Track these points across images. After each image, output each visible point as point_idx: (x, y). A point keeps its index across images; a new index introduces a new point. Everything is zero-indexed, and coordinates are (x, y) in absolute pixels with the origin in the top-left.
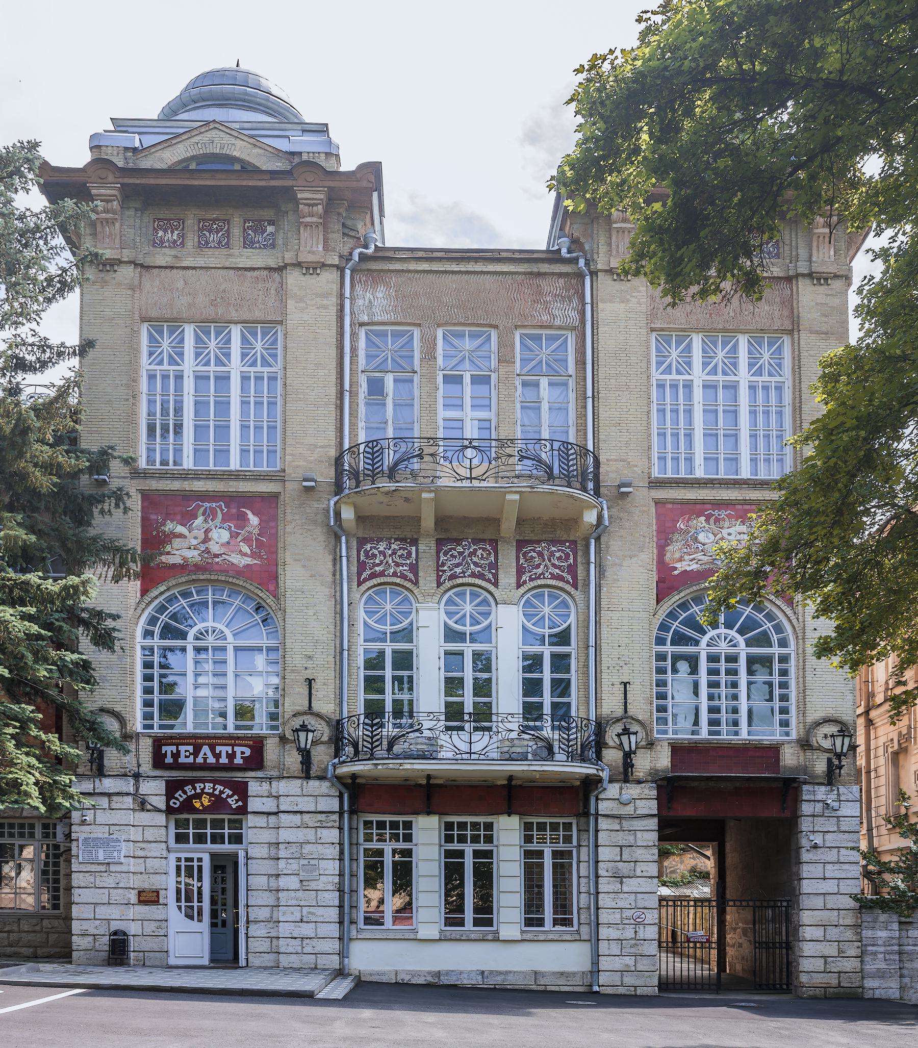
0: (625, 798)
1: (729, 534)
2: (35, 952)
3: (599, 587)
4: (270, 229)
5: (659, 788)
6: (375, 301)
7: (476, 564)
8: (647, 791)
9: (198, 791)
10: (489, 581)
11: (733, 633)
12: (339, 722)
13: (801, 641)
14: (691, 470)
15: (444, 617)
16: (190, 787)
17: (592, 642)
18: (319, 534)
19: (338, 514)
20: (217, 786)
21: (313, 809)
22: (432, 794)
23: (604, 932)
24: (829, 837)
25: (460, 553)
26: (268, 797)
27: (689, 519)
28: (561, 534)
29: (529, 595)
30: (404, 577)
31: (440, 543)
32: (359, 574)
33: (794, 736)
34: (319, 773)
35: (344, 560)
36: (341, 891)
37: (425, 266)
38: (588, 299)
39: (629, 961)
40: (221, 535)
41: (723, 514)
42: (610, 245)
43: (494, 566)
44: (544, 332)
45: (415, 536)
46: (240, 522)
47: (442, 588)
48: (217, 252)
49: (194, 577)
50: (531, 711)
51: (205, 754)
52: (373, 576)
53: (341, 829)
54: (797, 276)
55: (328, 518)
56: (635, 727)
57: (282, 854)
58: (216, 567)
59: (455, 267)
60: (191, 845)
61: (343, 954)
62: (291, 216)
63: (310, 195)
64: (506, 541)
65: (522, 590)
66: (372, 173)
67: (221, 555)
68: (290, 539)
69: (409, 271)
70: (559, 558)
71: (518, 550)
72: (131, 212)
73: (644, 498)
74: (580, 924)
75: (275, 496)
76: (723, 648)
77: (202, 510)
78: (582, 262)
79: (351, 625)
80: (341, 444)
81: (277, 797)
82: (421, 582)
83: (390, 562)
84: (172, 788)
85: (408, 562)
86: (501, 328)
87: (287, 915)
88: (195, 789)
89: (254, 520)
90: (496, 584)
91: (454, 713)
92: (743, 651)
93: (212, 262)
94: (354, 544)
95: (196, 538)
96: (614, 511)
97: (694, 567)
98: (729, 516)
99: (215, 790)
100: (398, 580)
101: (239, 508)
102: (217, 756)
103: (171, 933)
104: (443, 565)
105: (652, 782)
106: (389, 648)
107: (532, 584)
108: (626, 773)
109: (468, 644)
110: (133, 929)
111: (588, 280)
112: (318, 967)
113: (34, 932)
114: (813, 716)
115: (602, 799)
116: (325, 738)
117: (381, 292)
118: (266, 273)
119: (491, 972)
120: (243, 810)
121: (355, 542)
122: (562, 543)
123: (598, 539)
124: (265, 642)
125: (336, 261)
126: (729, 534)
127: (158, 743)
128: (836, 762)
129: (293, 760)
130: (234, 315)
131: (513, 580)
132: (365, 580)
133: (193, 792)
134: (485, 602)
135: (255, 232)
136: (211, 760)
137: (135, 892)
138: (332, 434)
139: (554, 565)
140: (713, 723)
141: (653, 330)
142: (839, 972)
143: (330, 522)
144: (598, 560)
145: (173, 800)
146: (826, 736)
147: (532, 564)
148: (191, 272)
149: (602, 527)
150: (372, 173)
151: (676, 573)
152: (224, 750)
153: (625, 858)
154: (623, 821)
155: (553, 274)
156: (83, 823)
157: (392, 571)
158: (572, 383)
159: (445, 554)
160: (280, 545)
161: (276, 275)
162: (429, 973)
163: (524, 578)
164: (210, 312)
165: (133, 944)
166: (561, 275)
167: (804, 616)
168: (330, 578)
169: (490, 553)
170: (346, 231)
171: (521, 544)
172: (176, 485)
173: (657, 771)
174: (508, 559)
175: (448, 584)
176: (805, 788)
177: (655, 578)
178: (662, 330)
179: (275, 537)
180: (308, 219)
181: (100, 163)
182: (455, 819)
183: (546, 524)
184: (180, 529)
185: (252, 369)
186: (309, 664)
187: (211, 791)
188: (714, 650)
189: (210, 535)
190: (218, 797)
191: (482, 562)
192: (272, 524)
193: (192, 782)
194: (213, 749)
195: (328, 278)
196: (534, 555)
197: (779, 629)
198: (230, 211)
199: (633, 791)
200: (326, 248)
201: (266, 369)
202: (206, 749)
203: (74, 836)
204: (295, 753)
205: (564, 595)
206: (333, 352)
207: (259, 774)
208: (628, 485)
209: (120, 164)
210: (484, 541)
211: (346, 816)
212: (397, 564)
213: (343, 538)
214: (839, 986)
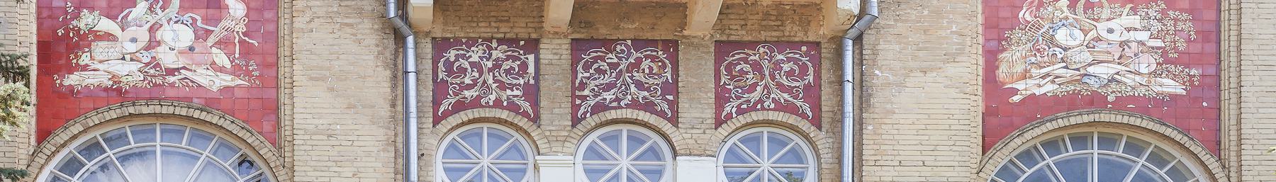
7: (640, 85)
10: (662, 114)
25: (613, 66)
29: (735, 139)
30: (513, 107)
31: (578, 46)
32: (436, 103)
40: (177, 35)
43: (672, 88)
45: (534, 36)
46: (211, 11)
49: (131, 110)
52: (460, 107)
58: (171, 93)
64: (694, 44)
65: (724, 130)
67: (178, 70)
68: (301, 42)
70: (790, 74)
71: (718, 63)
82: (545, 116)
83: (490, 81)
90: (674, 121)
100: (504, 115)
104: (583, 86)
107: (742, 120)
122: (795, 45)
123: (858, 40)
131: (709, 114)
132: (446, 114)
134: (654, 153)
139: (781, 87)
144: (857, 76)
147: (741, 84)
149: (867, 18)
157: (493, 97)
163: (728, 109)
169: (664, 66)
171: (723, 48)
174: (698, 75)
179: (275, 37)
189: (159, 35)
191: (651, 81)
192: (269, 15)
196: (747, 68)
205: (797, 139)
210: (653, 43)
212: (502, 86)
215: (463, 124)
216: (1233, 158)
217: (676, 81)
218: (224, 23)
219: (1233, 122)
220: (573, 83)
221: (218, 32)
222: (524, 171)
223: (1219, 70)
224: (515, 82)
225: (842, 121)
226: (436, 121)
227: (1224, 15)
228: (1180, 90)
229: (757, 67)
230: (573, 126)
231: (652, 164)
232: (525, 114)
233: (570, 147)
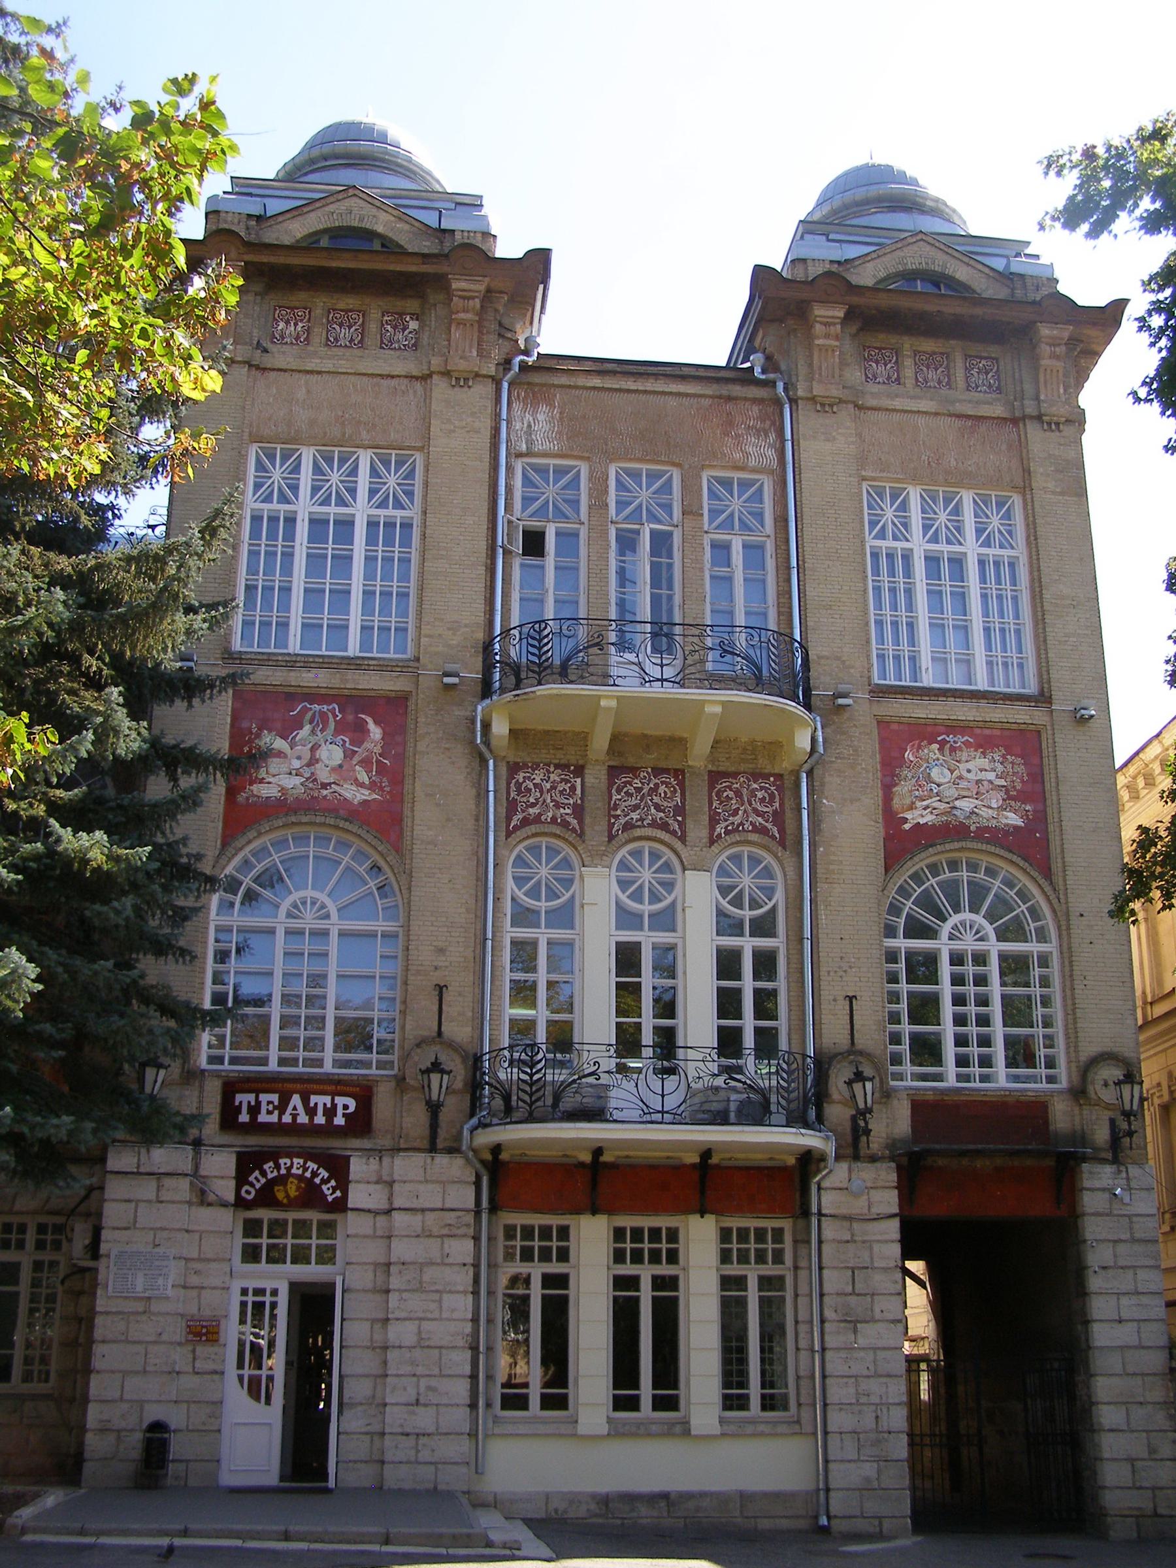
1: (969, 771)
4: (413, 325)
5: (899, 1169)
6: (536, 425)
8: (883, 1174)
9: (283, 1171)
10: (674, 833)
12: (478, 1059)
13: (1064, 933)
15: (615, 888)
16: (271, 1164)
20: (309, 1164)
21: (439, 1205)
22: (598, 1182)
25: (638, 790)
26: (377, 1183)
27: (919, 747)
28: (764, 765)
33: (1064, 1083)
34: (447, 1144)
35: (491, 794)
37: (596, 382)
39: (869, 1470)
40: (331, 754)
41: (961, 739)
42: (811, 365)
43: (680, 810)
44: (736, 475)
45: (581, 762)
48: (348, 352)
49: (294, 819)
50: (728, 1042)
51: (295, 1108)
52: (525, 822)
53: (476, 1239)
57: (395, 1282)
59: (631, 384)
65: (715, 849)
67: (330, 784)
69: (576, 387)
70: (762, 800)
71: (711, 787)
74: (799, 1405)
76: (968, 944)
77: (310, 714)
79: (497, 900)
83: (549, 801)
84: (247, 1164)
85: (571, 802)
86: (687, 466)
88: (278, 1167)
89: (375, 732)
90: (683, 839)
91: (628, 1042)
92: (994, 948)
93: (343, 365)
94: (504, 770)
95: (299, 758)
96: (828, 730)
97: (928, 818)
99: (306, 1169)
100: (557, 830)
101: (357, 713)
102: (311, 1112)
104: (616, 807)
105: (892, 1158)
108: (854, 1145)
111: (787, 406)
112: (439, 1487)
115: (826, 1189)
118: (406, 381)
120: (340, 1206)
121: (505, 769)
122: (766, 777)
124: (380, 925)
126: (969, 771)
127: (231, 1088)
131: (705, 833)
132: (516, 828)
133: (275, 1173)
134: (667, 867)
135: (395, 327)
136: (303, 1119)
139: (755, 811)
140: (962, 1061)
143: (475, 737)
145: (246, 1187)
146: (1106, 1085)
148: (315, 377)
151: (907, 826)
152: (320, 1101)
154: (855, 1225)
155: (746, 399)
157: (550, 814)
159: (619, 791)
160: (408, 771)
161: (418, 385)
166: (754, 401)
167: (1066, 894)
168: (470, 824)
170: (503, 331)
174: (698, 799)
177: (882, 834)
179: (400, 758)
182: (628, 1221)
183: (745, 749)
184: (280, 744)
187: (300, 1172)
188: (957, 945)
189: (318, 753)
191: (665, 804)
192: (399, 739)
193: (274, 1156)
195: (483, 390)
196: (731, 794)
197: (1035, 913)
198: (367, 300)
199: (866, 1173)
202: (296, 1100)
203: (104, 1248)
206: (485, 493)
207: (366, 1143)
210: (666, 771)
211: (485, 1216)
212: (558, 805)
213: (491, 762)
215: (528, 837)
216: (1061, 882)
217: (683, 803)
218: (367, 745)
219: (1058, 850)
220: (609, 803)
222: (571, 881)
223: (1045, 806)
224: (566, 801)
226: (509, 834)
227: (1045, 760)
229: (738, 794)
230: (610, 841)
232: (574, 830)
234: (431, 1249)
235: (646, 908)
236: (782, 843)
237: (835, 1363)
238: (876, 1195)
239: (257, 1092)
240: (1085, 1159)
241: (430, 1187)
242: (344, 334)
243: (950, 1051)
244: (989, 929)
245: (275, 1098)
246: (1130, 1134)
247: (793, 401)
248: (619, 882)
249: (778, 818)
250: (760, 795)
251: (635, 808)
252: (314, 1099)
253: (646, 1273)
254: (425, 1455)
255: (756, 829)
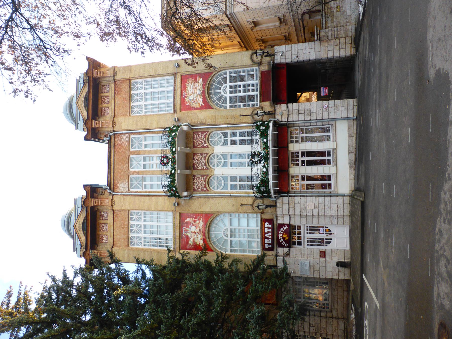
0: (281, 114)
2: (346, 291)
3: (208, 125)
4: (102, 213)
5: (277, 104)
6: (122, 187)
10: (206, 155)
11: (222, 87)
14: (171, 103)
15: (219, 167)
17: (227, 126)
18: (192, 202)
19: (186, 196)
23: (332, 116)
24: (293, 53)
25: (198, 163)
31: (194, 168)
33: (258, 68)
36: (318, 196)
37: (112, 174)
38: (121, 132)
39: (343, 108)
40: (193, 229)
41: (184, 93)
43: (202, 154)
44: (131, 143)
47: (209, 168)
52: (205, 187)
53: (294, 196)
54: (114, 79)
55: (187, 199)
56: (256, 112)
57: (305, 214)
58: (204, 230)
60: (302, 241)
61: (343, 195)
62: (99, 207)
63: (92, 203)
65: (209, 146)
66: (85, 186)
71: (197, 148)
72: (98, 248)
73: (179, 114)
74: (329, 124)
75: (180, 214)
76: (228, 90)
78: (111, 134)
79: (222, 193)
80: (164, 196)
81: (283, 215)
82: (207, 174)
84: (280, 245)
87: (328, 213)
88: (281, 239)
89: (188, 220)
90: (208, 153)
93: (112, 228)
94: (195, 192)
97: (201, 100)
98: (185, 91)
102: (269, 232)
103: (337, 248)
105: (275, 106)
106: (229, 183)
108: (272, 114)
109: (228, 161)
110: (335, 260)
111: (115, 132)
113: (337, 290)
114: (250, 62)
116: (262, 201)
117: (119, 185)
119: (349, 150)
120: (289, 225)
122: (194, 136)
125: (111, 197)
128: (266, 54)
129: (269, 210)
130: (127, 223)
131: (206, 149)
134: (214, 156)
136: (270, 234)
137: (321, 259)
138: (161, 198)
139: (201, 137)
140: (253, 90)
141: (130, 115)
142: (346, 44)
146: (257, 58)
150: (85, 186)
152: (266, 230)
153: (303, 112)
156: (294, 272)
158: (145, 135)
160: (196, 212)
161: (115, 212)
162: (350, 169)
164: (126, 229)
165: (342, 260)
166: (114, 139)
168: (207, 199)
172: (178, 241)
173: (271, 105)
175: (208, 166)
176: (276, 62)
178: (130, 113)
180: (99, 203)
181: (84, 255)
184: (191, 240)
185: (142, 219)
186: (236, 205)
188: (228, 92)
190: (284, 232)
193: (278, 240)
194: (266, 233)
195: (115, 198)
199: (278, 111)
200: (107, 199)
201: (142, 215)
202: (266, 235)
203: (299, 276)
204: (267, 209)
206: (137, 197)
207: (275, 220)
208: (175, 119)
209: (85, 250)
214: (351, 43)
218: (191, 221)
221: (192, 222)
225: (207, 128)
228: (201, 79)
231: (216, 157)
233: (213, 170)
234: (297, 206)
235: (223, 161)
236: (208, 132)
237: (319, 117)
238: (283, 109)
239: (265, 244)
240: (274, 62)
241: (284, 206)
242: (105, 227)
243: (251, 93)
244: (225, 85)
245: (266, 240)
246: (268, 52)
247: (114, 131)
248: (218, 166)
249: (202, 133)
250: (198, 137)
251: (201, 164)
252: (266, 232)
253: (301, 159)
254: (342, 206)
255: (205, 137)
